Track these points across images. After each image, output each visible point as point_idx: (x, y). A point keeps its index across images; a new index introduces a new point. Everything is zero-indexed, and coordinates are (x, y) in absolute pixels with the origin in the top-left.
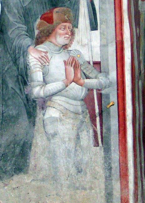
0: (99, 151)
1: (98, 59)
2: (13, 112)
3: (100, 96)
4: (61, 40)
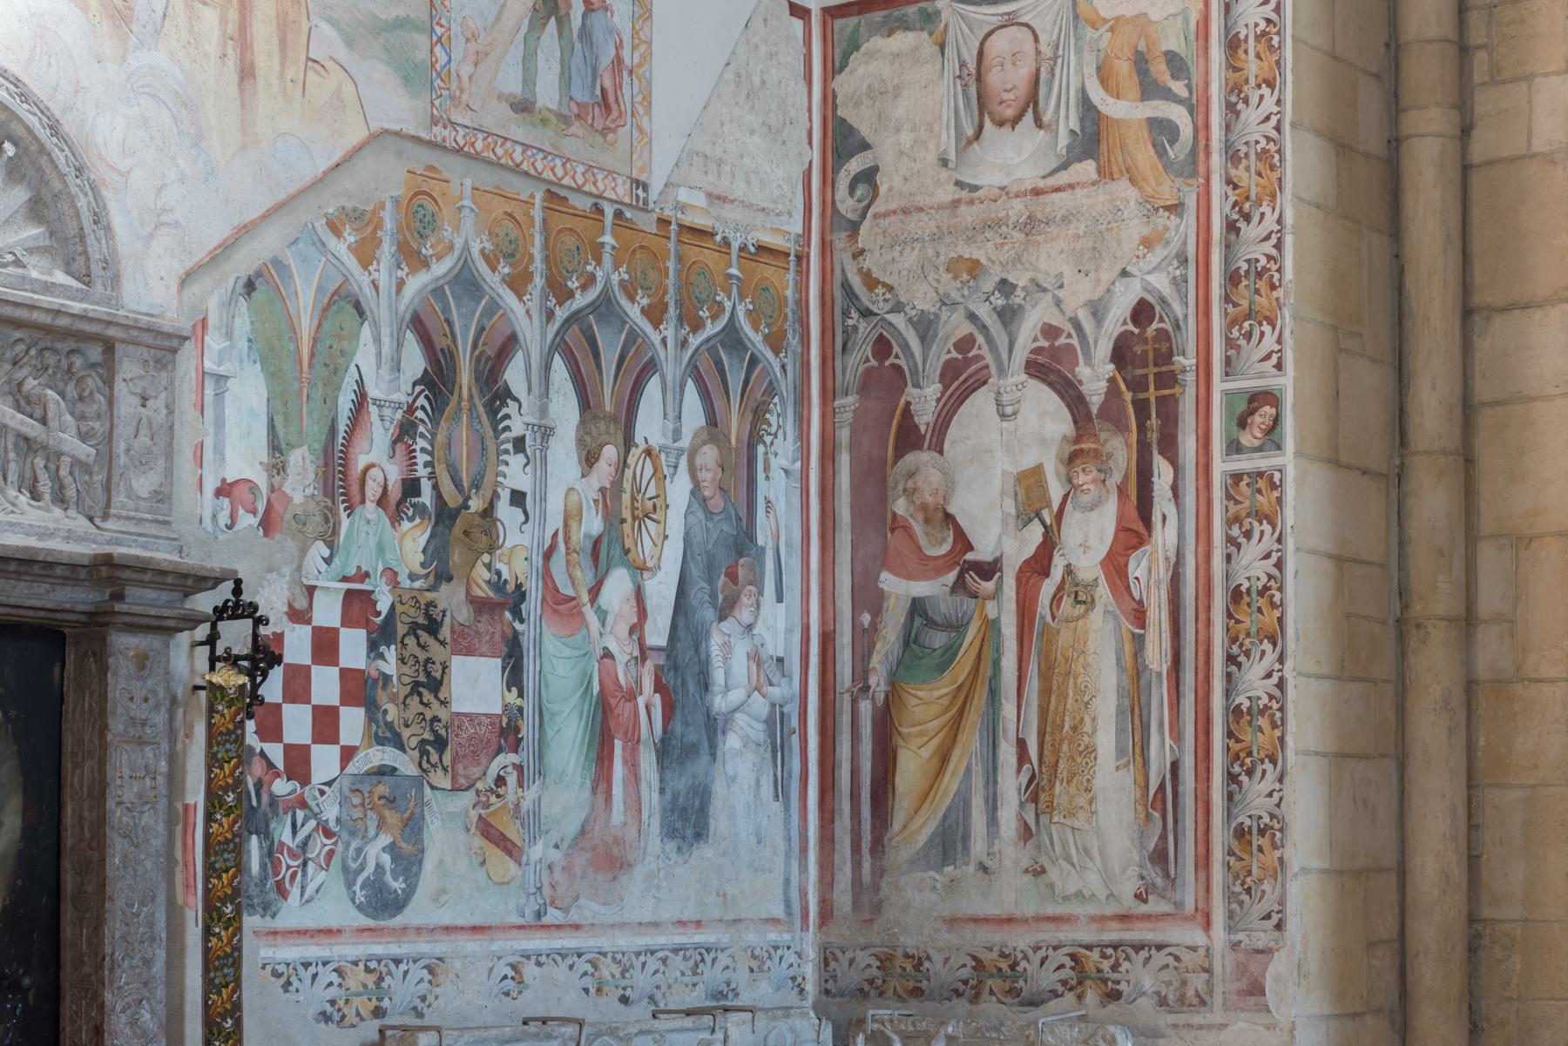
0: (777, 806)
1: (781, 654)
2: (692, 737)
3: (782, 714)
4: (745, 615)
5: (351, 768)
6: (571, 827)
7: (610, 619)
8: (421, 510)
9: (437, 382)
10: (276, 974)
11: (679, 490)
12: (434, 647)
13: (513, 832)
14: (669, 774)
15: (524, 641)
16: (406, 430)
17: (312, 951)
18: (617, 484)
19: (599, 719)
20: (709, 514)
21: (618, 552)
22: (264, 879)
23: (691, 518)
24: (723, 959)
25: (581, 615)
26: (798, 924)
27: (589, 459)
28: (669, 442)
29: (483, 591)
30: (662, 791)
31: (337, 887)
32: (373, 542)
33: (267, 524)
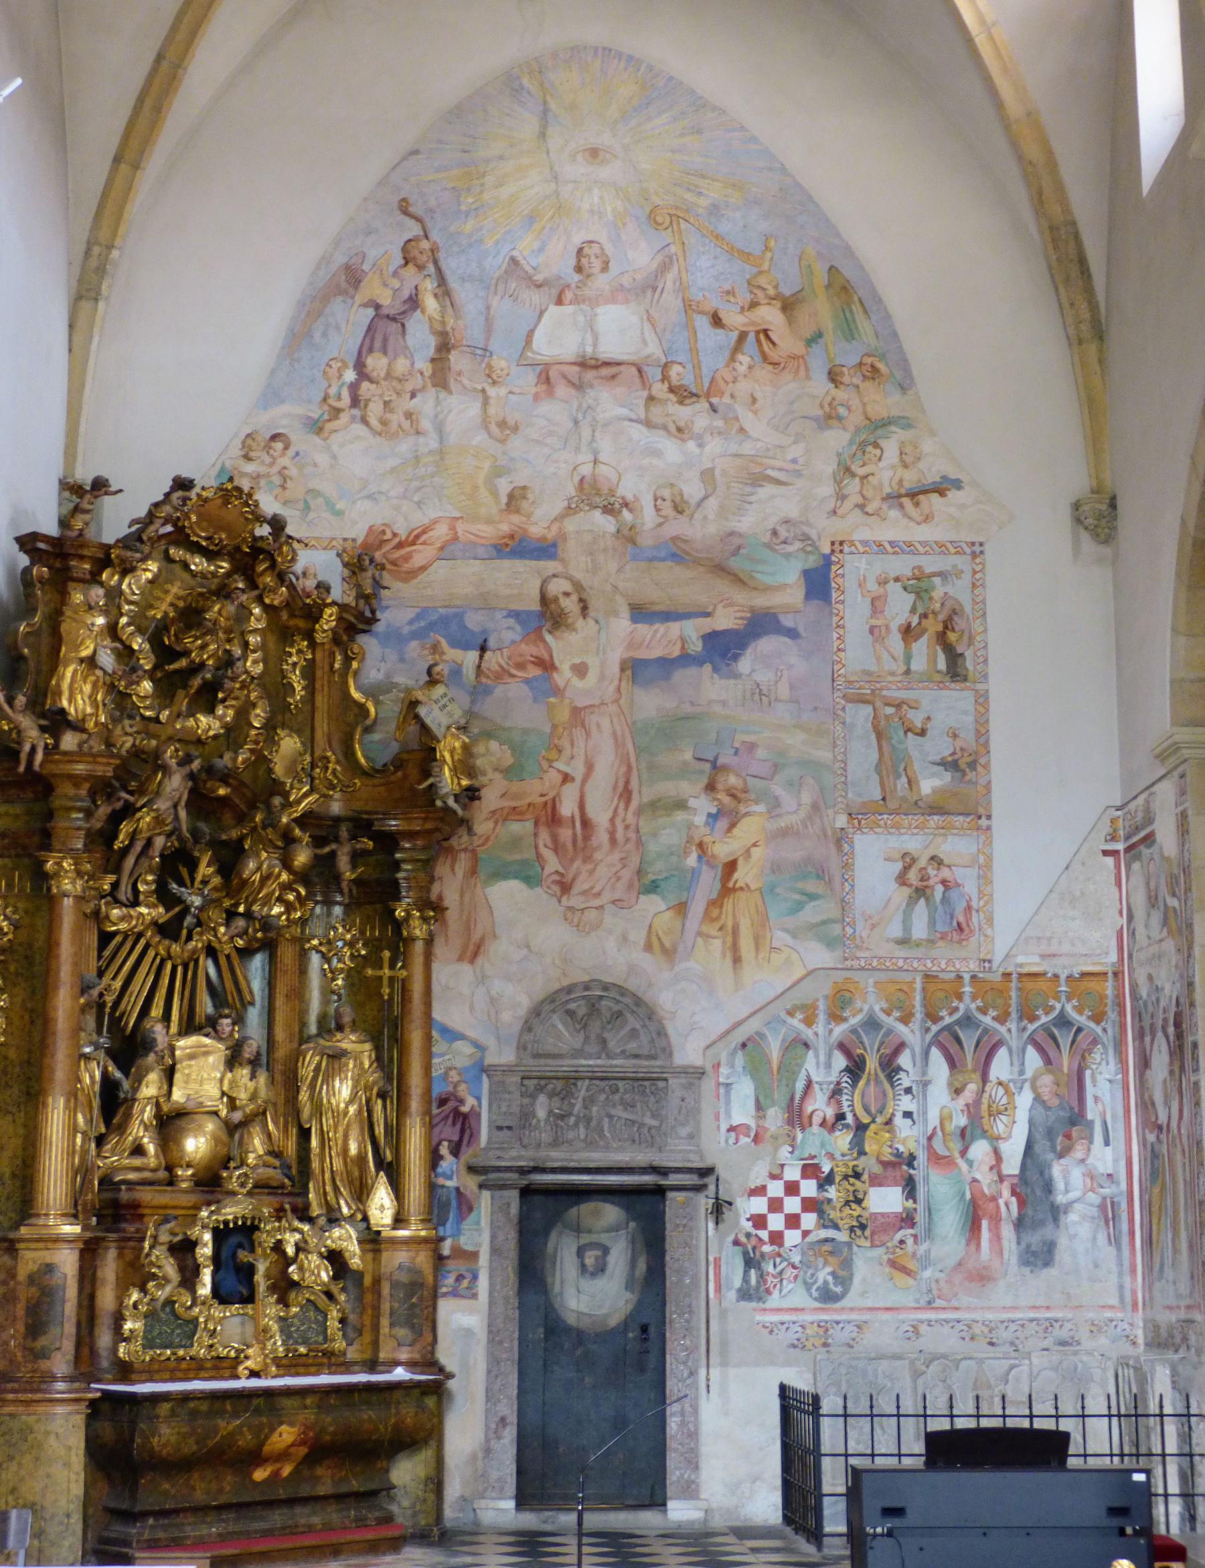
0: (1111, 1251)
1: (1110, 1172)
2: (1040, 1216)
3: (1113, 1203)
4: (1078, 1153)
5: (808, 1239)
6: (951, 1262)
7: (975, 1165)
8: (847, 1126)
9: (855, 1069)
10: (765, 1327)
11: (1024, 1100)
12: (858, 1183)
13: (912, 1265)
14: (1023, 1235)
15: (917, 1179)
16: (836, 1092)
17: (786, 1317)
18: (978, 1102)
19: (971, 1209)
20: (1048, 1108)
21: (979, 1132)
22: (757, 1288)
23: (1034, 1112)
24: (1068, 1326)
25: (956, 1164)
26: (1129, 1308)
27: (958, 1092)
28: (1015, 1076)
29: (888, 1157)
30: (1019, 1243)
31: (801, 1290)
32: (818, 1143)
33: (757, 1139)
